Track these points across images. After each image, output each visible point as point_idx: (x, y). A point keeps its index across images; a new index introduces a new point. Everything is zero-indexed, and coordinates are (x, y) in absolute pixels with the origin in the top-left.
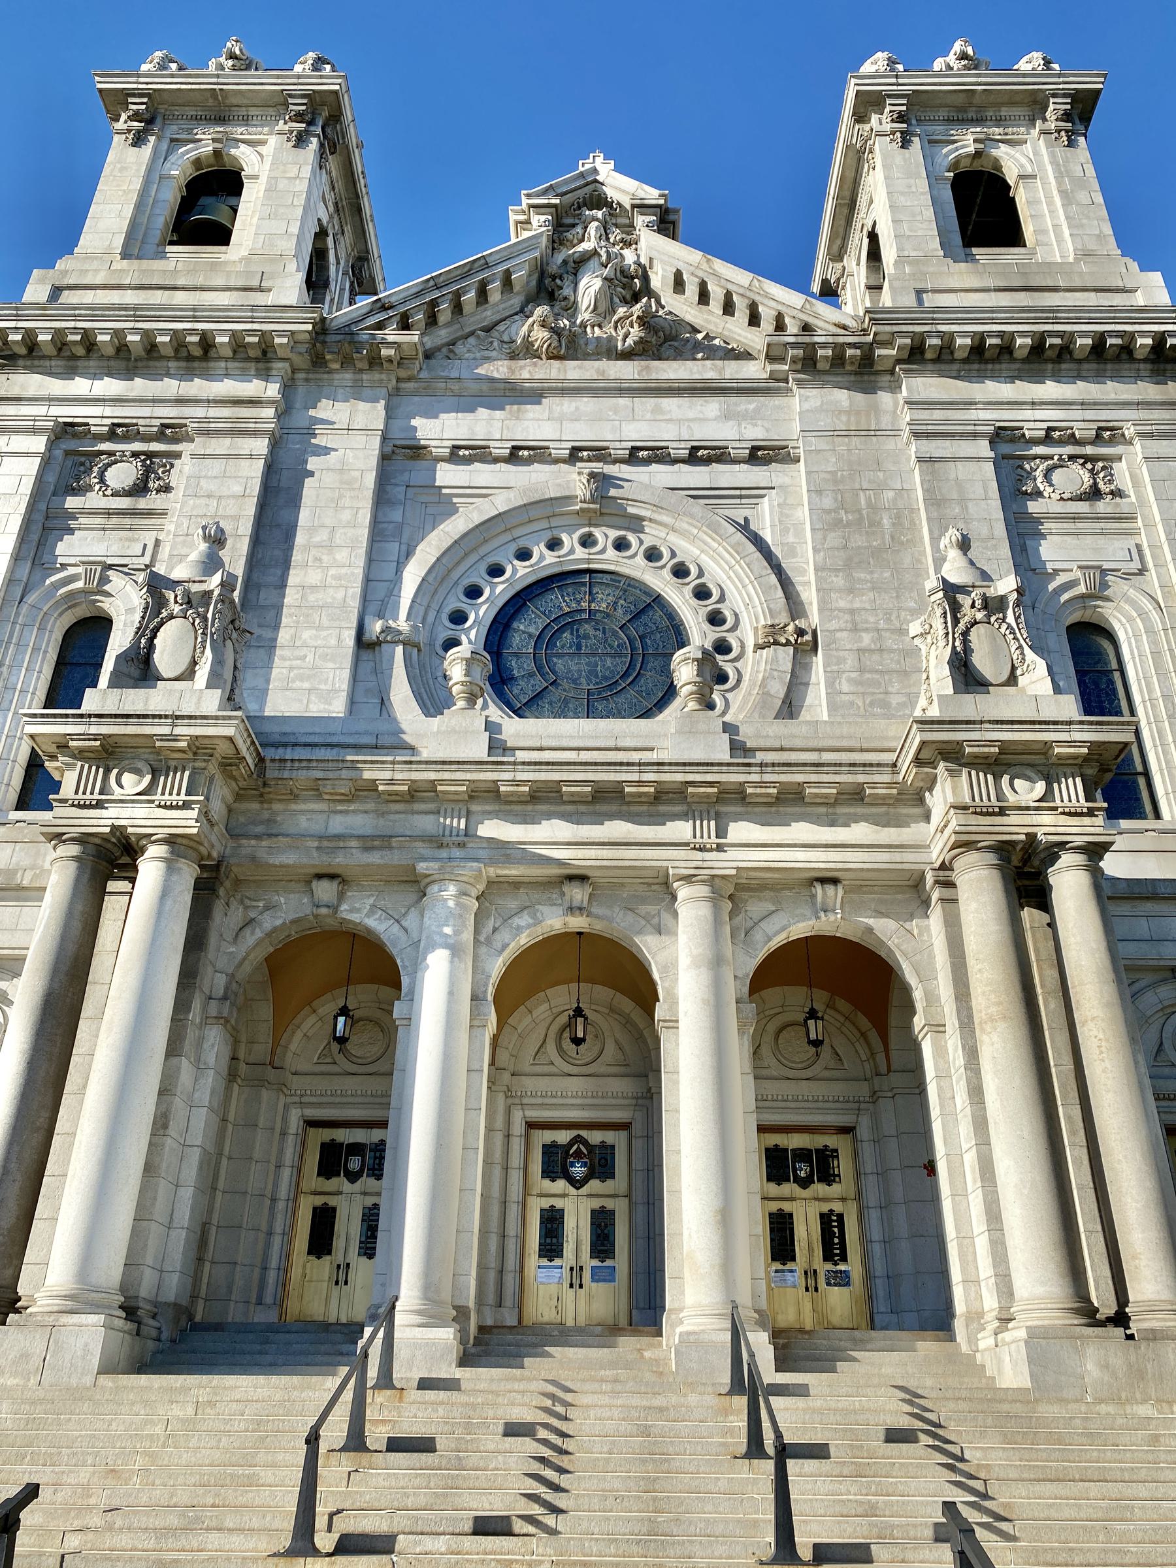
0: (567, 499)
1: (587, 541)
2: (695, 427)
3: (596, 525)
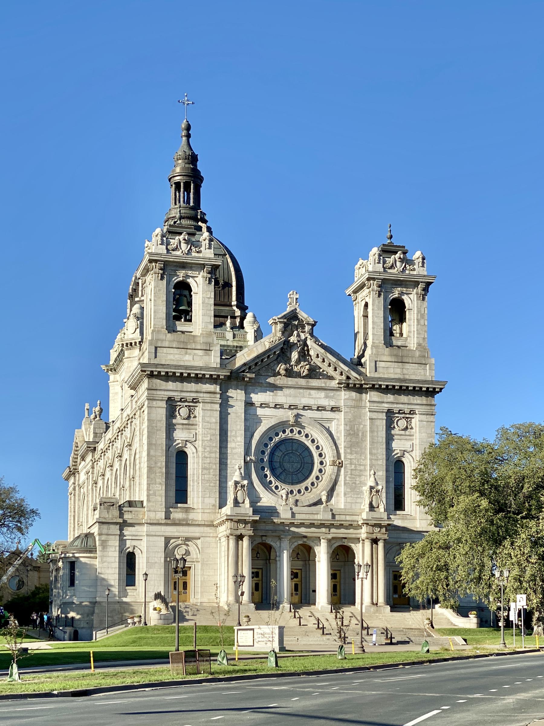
1: (292, 431)
2: (319, 400)
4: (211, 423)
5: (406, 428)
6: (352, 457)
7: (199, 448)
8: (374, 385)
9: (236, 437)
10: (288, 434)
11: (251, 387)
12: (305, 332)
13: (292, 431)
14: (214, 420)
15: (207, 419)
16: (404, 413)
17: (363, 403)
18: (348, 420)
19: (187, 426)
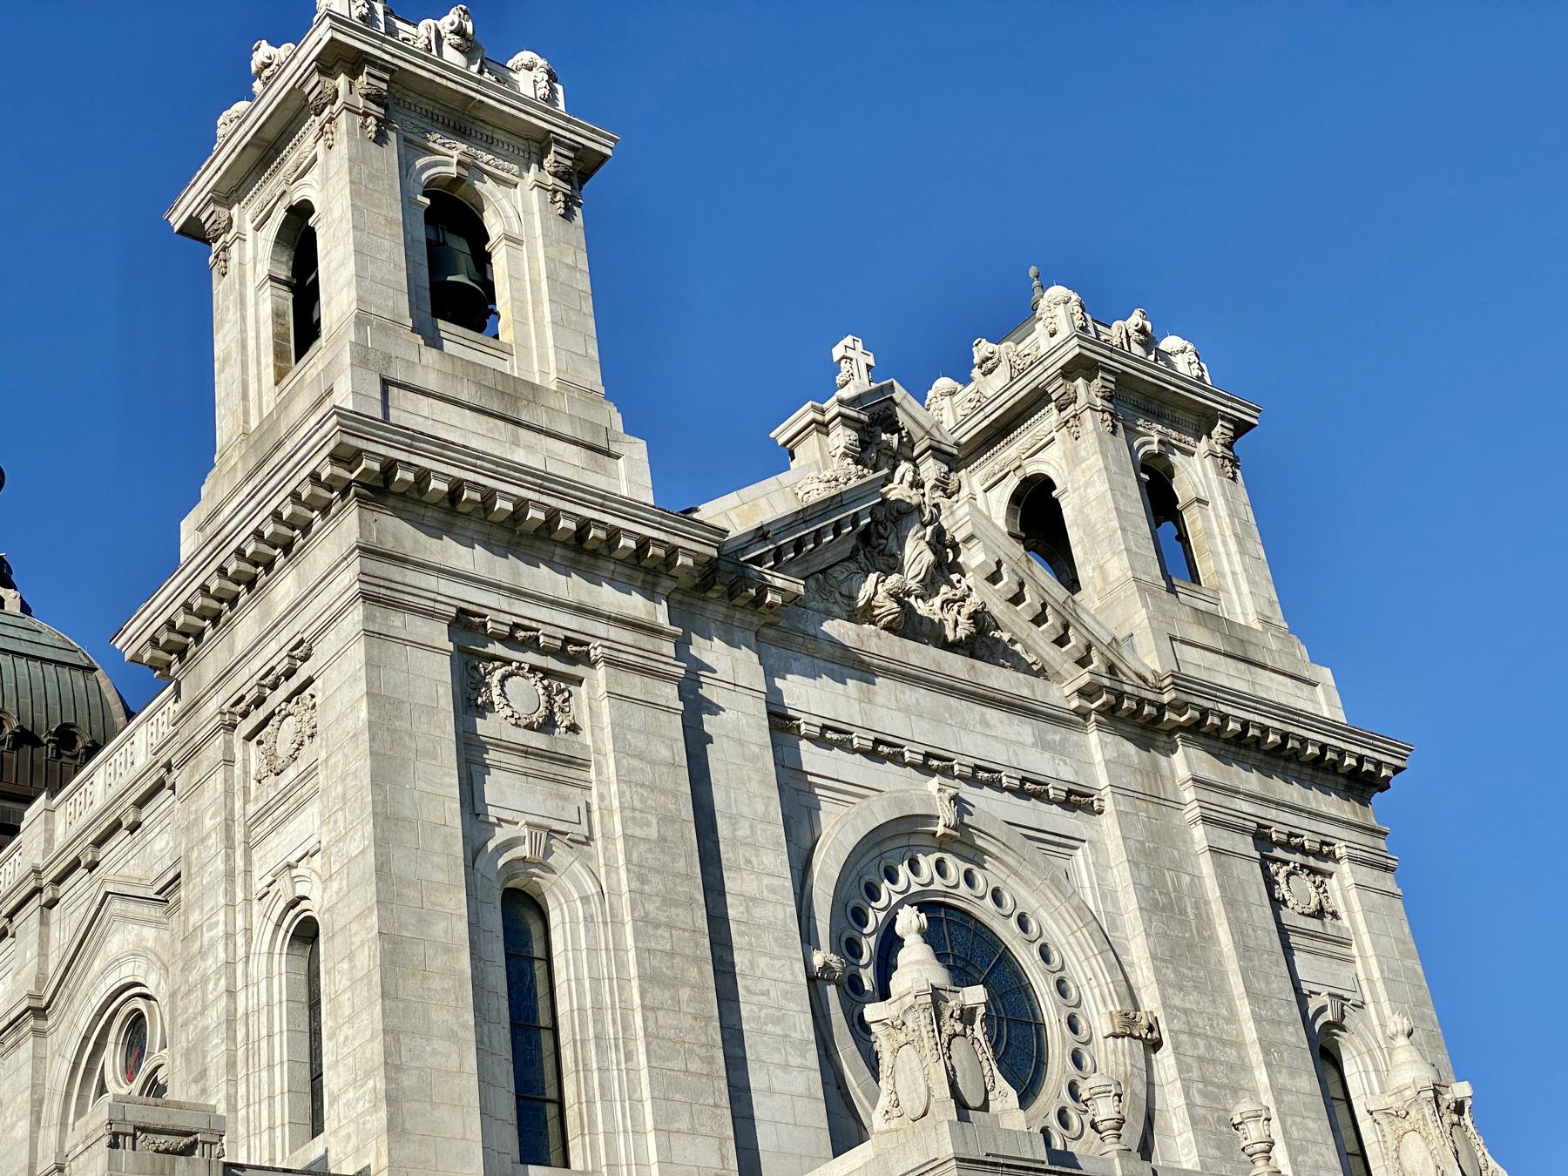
0: (931, 818)
1: (940, 867)
2: (1020, 751)
3: (946, 851)
4: (652, 762)
5: (1320, 913)
6: (1188, 1006)
7: (614, 876)
8: (1205, 712)
9: (756, 848)
10: (932, 882)
11: (774, 649)
12: (923, 486)
13: (940, 867)
14: (665, 753)
15: (638, 742)
16: (1301, 849)
17: (1169, 786)
18: (1139, 846)
19: (545, 766)
